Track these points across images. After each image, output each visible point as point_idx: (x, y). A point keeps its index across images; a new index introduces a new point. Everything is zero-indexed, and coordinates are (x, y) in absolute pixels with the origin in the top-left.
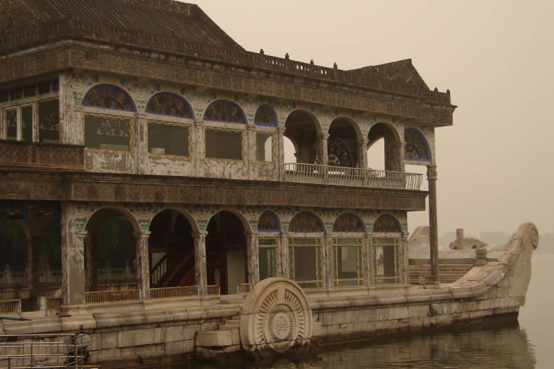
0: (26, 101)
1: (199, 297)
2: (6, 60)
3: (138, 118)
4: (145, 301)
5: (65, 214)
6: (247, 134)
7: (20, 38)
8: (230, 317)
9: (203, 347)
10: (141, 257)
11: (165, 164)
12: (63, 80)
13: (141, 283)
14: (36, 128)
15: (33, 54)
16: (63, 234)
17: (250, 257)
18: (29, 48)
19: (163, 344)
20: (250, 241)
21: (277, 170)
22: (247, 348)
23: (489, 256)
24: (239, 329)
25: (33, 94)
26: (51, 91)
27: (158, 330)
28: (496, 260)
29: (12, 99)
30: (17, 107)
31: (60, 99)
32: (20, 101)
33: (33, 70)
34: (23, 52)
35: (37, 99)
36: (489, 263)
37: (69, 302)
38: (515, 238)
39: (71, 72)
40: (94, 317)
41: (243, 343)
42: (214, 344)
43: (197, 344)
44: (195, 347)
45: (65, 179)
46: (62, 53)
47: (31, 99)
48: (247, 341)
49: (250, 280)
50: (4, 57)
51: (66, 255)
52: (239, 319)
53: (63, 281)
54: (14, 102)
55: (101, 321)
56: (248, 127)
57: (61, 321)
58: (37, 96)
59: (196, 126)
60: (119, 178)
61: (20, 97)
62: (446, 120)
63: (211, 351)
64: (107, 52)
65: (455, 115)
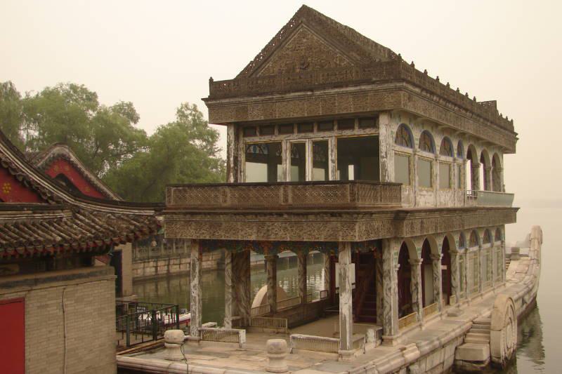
0: (319, 136)
1: (440, 313)
2: (311, 96)
3: (415, 154)
4: (423, 323)
5: (389, 250)
6: (454, 166)
7: (328, 75)
8: (468, 331)
9: (466, 361)
10: (417, 283)
11: (424, 195)
12: (383, 120)
13: (418, 306)
14: (333, 161)
15: (351, 93)
16: (385, 267)
17: (455, 272)
18: (347, 86)
19: (443, 363)
20: (455, 259)
21: (463, 196)
22: (497, 360)
23: (521, 253)
24: (489, 343)
25: (331, 129)
26: (356, 127)
27: (443, 350)
28: (527, 256)
29: (299, 132)
30: (307, 140)
31: (381, 138)
32: (311, 135)
33: (348, 107)
34: (337, 90)
35: (336, 135)
36: (522, 258)
37: (393, 333)
38: (532, 237)
39: (389, 112)
40: (418, 347)
41: (493, 355)
42: (478, 360)
43: (458, 358)
44: (455, 360)
45: (399, 217)
46: (392, 94)
47: (327, 134)
48: (498, 353)
49: (453, 292)
50: (309, 93)
51: (390, 289)
52: (489, 333)
53: (385, 313)
54: (303, 135)
55: (423, 349)
56: (455, 160)
57: (403, 355)
58: (336, 131)
59: (436, 160)
60: (423, 214)
61: (312, 131)
62: (513, 151)
63: (474, 365)
64: (417, 94)
65: (518, 145)
